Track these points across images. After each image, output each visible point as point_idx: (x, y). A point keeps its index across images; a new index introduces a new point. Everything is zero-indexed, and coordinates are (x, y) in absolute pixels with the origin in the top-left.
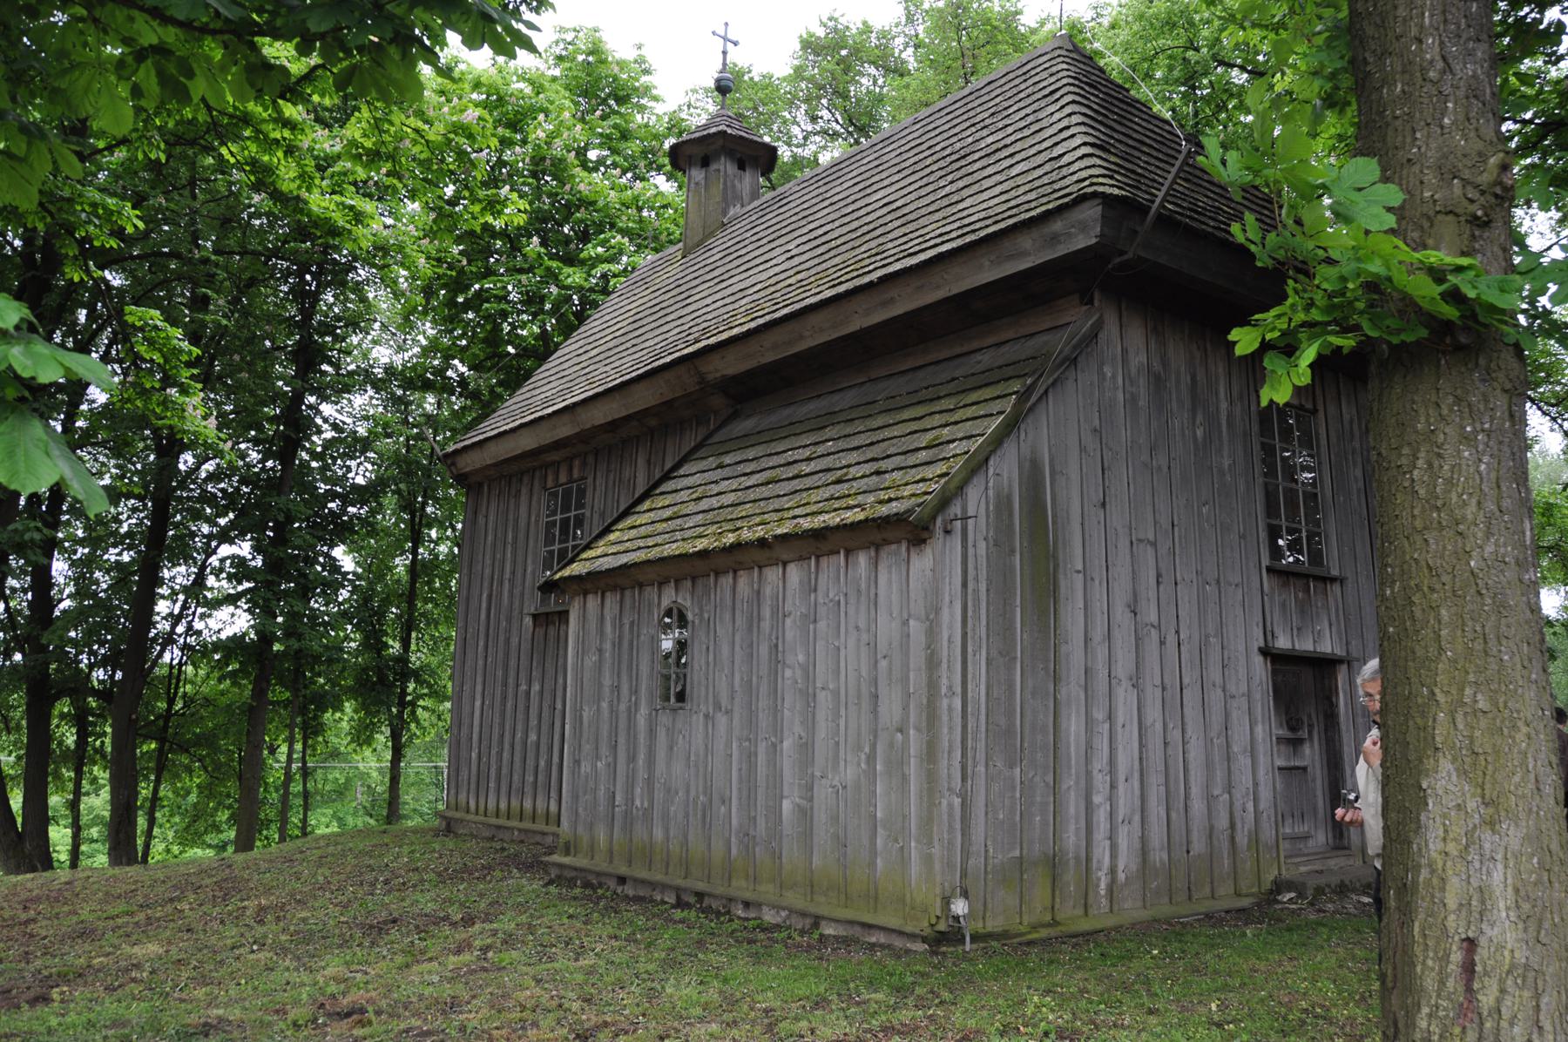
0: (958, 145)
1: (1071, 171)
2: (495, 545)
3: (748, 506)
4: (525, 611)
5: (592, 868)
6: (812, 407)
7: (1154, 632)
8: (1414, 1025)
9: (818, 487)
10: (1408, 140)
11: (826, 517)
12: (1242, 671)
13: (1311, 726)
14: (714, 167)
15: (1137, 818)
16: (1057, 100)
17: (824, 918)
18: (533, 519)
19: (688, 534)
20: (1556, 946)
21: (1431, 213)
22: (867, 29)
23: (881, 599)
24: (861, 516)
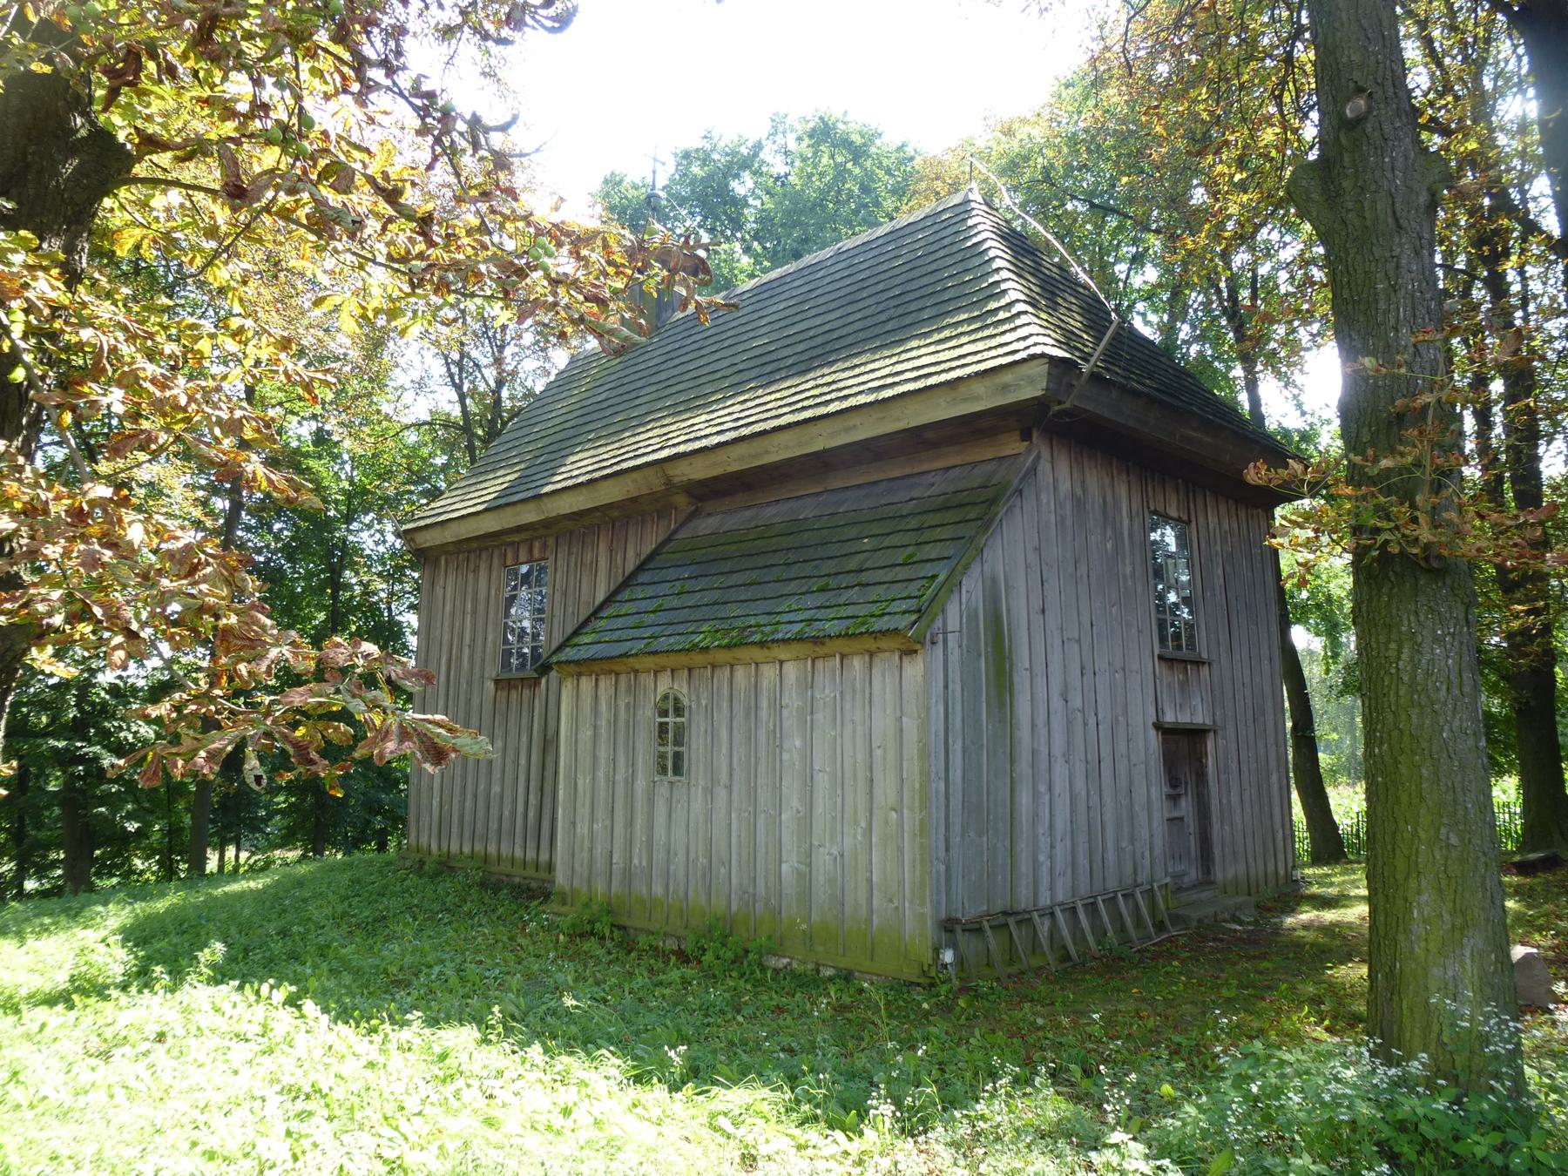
2: (453, 614)
12: (1141, 744)
15: (1069, 871)
23: (876, 698)
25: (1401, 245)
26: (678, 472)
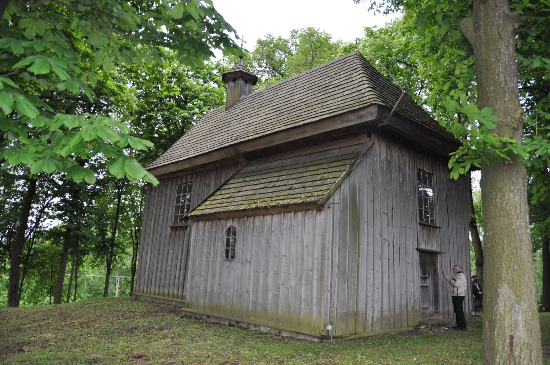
0: (324, 83)
1: (365, 95)
3: (258, 195)
4: (168, 225)
5: (198, 313)
6: (275, 164)
7: (387, 242)
8: (495, 361)
9: (282, 191)
10: (495, 103)
11: (288, 201)
12: (411, 256)
13: (429, 273)
14: (237, 82)
15: (380, 301)
16: (357, 72)
17: (283, 330)
18: (172, 195)
19: (237, 203)
20: (536, 338)
21: (502, 125)
22: (280, 39)
24: (301, 201)
25: (501, 44)
26: (241, 149)
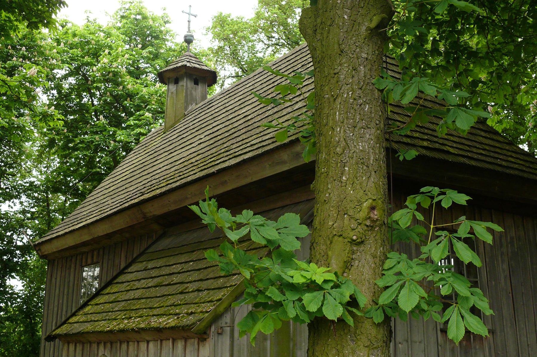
9: (173, 294)
14: (181, 83)
